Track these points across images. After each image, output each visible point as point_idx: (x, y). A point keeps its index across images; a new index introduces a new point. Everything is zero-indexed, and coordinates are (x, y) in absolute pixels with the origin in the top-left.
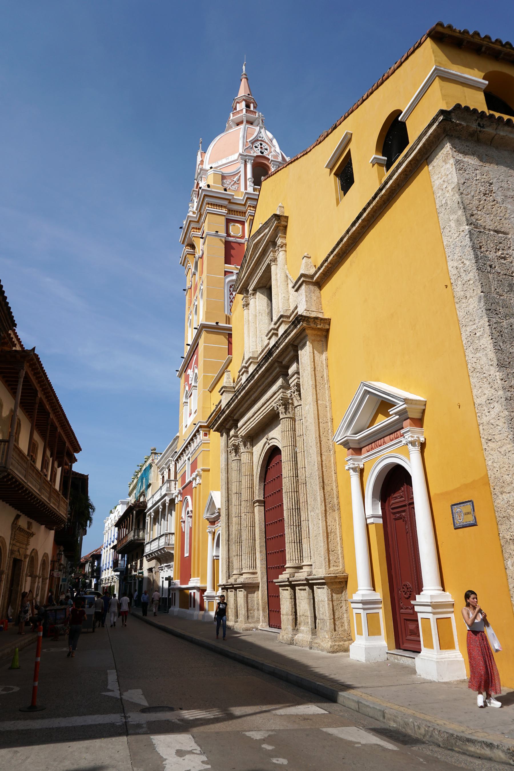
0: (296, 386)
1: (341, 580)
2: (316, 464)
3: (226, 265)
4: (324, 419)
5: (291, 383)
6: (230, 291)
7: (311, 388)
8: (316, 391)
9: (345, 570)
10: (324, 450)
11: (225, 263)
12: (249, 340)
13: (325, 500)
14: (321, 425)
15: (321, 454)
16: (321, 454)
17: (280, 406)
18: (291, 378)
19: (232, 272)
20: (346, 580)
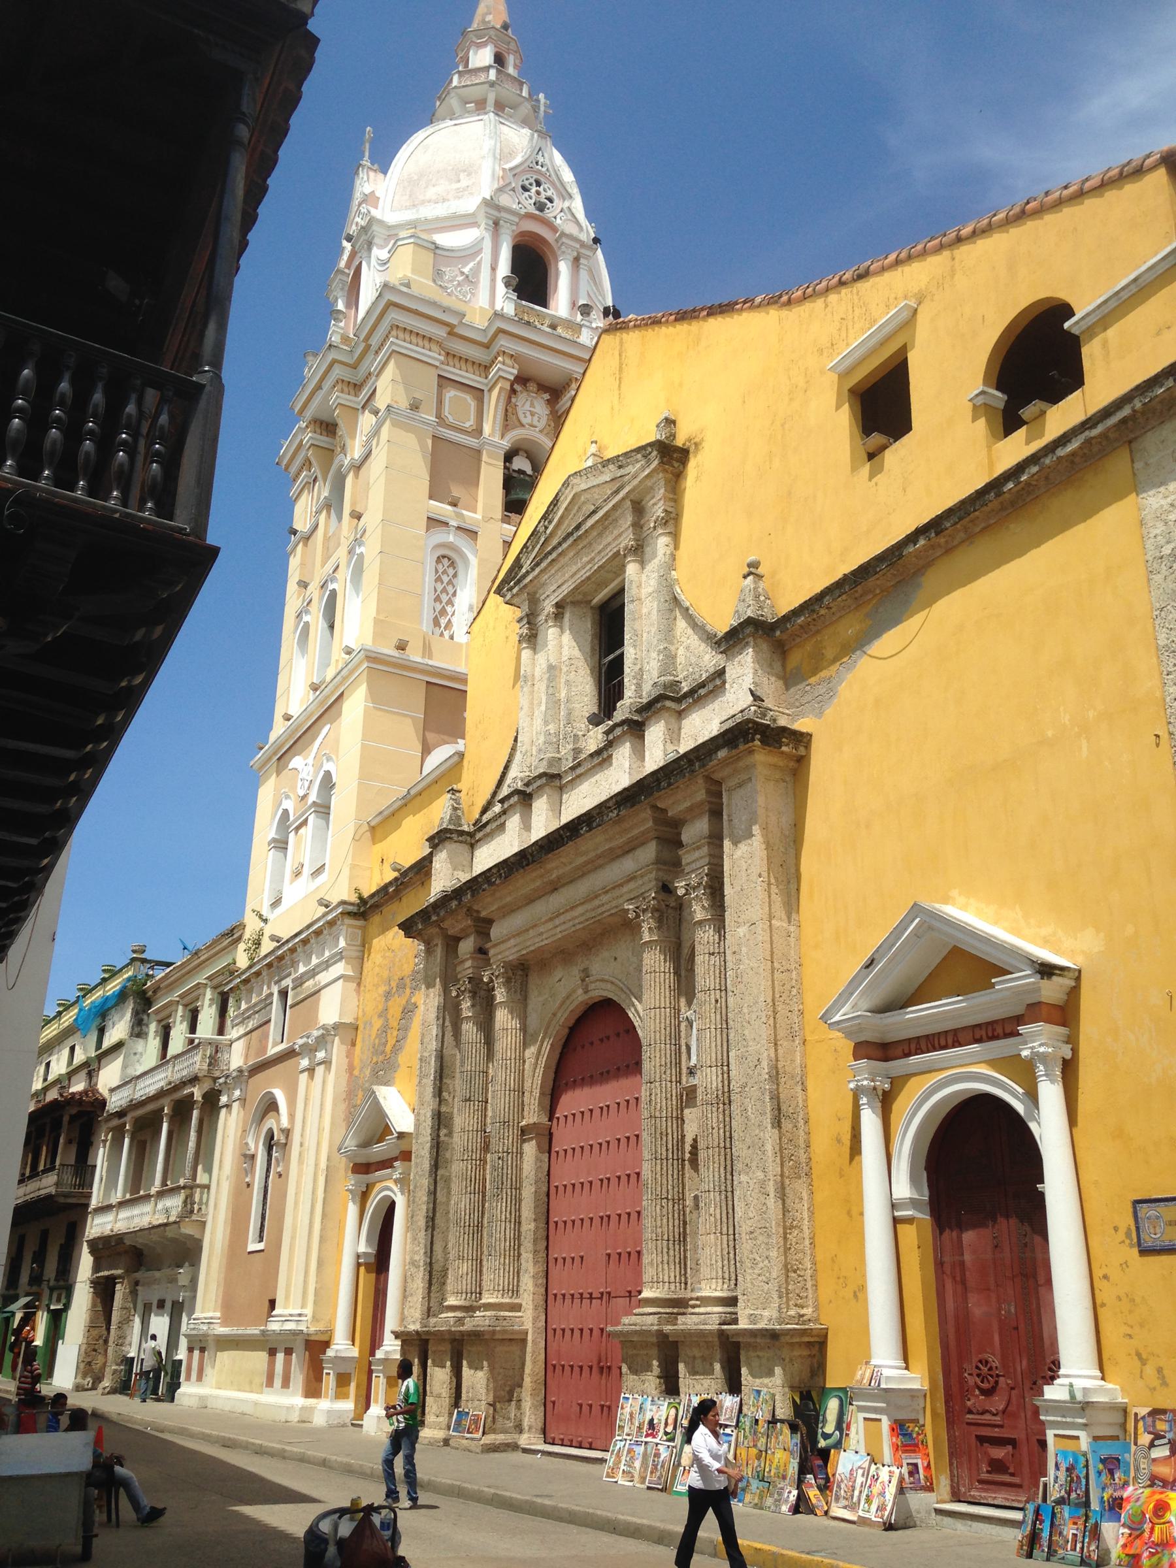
0: (707, 875)
1: (812, 1340)
2: (765, 1064)
3: (432, 502)
4: (784, 963)
5: (688, 864)
6: (437, 571)
7: (759, 888)
8: (770, 897)
9: (819, 1315)
10: (782, 1035)
11: (431, 498)
12: (532, 725)
13: (781, 1150)
14: (776, 974)
15: (776, 1044)
16: (776, 1044)
17: (644, 911)
18: (688, 852)
19: (446, 524)
20: (822, 1340)
